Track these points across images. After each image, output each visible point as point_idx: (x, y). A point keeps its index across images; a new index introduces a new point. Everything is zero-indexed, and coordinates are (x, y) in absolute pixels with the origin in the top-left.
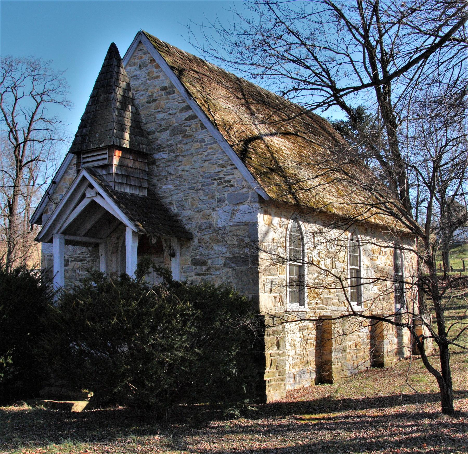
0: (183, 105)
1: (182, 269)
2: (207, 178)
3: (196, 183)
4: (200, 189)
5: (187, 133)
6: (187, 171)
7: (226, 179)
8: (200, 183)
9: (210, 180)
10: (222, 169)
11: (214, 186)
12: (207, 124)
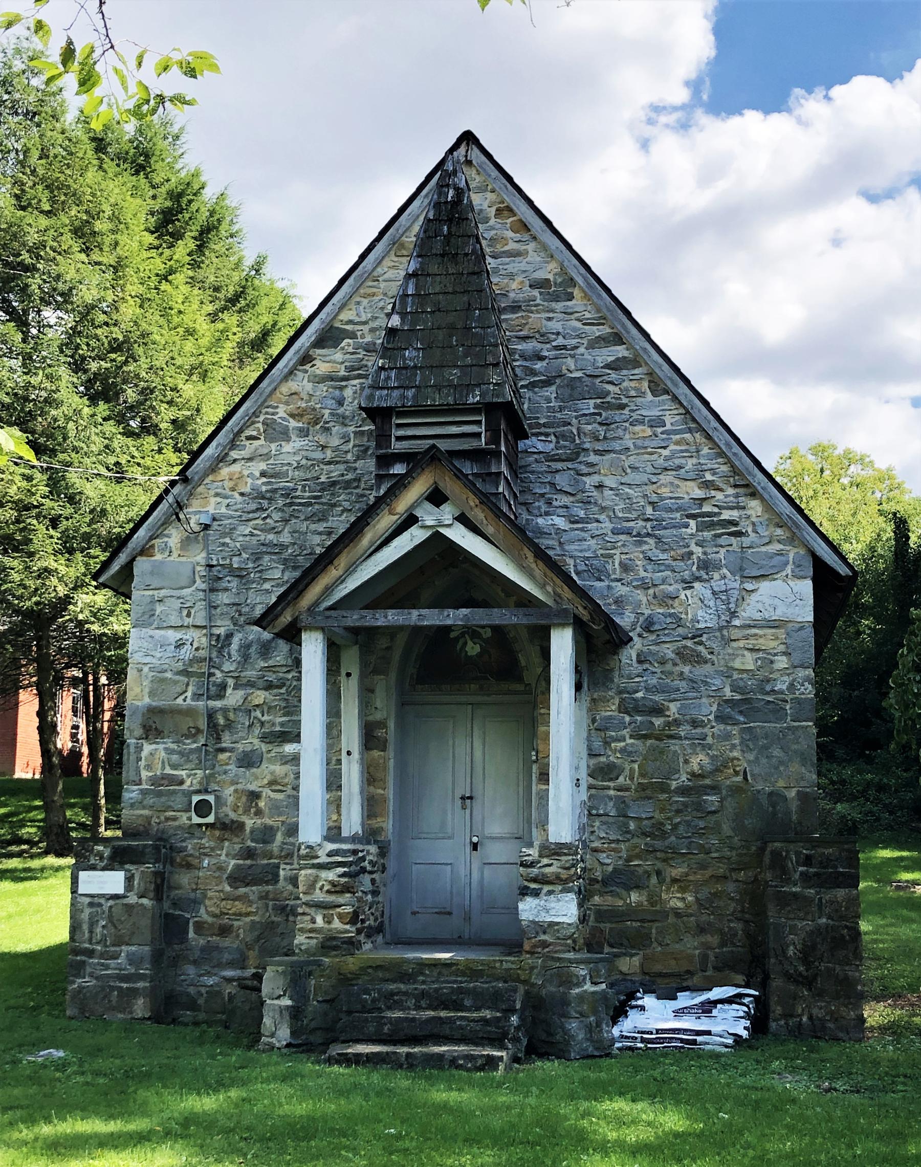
0: (605, 330)
1: (594, 721)
2: (670, 510)
3: (636, 519)
4: (648, 535)
5: (608, 399)
6: (611, 489)
7: (722, 517)
8: (648, 520)
9: (678, 515)
10: (713, 493)
11: (689, 531)
12: (676, 385)
